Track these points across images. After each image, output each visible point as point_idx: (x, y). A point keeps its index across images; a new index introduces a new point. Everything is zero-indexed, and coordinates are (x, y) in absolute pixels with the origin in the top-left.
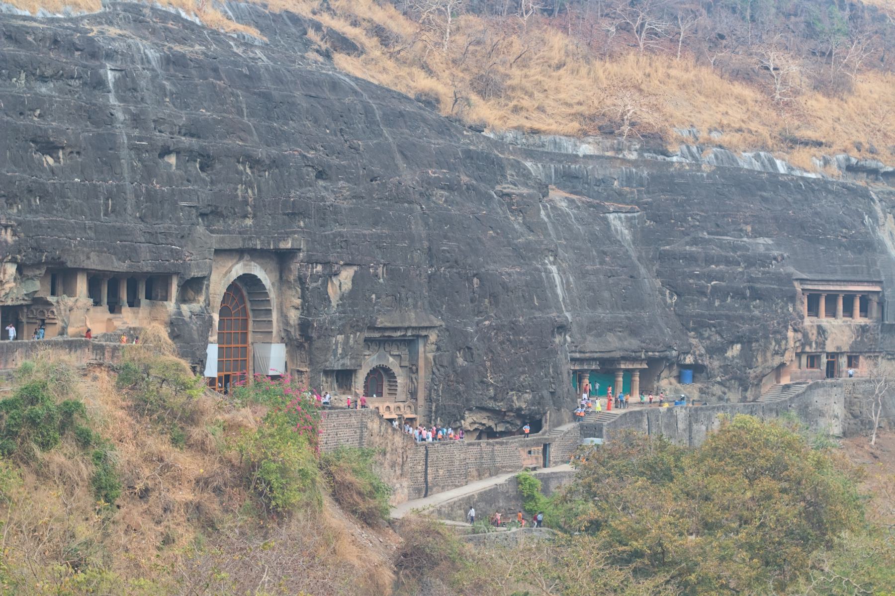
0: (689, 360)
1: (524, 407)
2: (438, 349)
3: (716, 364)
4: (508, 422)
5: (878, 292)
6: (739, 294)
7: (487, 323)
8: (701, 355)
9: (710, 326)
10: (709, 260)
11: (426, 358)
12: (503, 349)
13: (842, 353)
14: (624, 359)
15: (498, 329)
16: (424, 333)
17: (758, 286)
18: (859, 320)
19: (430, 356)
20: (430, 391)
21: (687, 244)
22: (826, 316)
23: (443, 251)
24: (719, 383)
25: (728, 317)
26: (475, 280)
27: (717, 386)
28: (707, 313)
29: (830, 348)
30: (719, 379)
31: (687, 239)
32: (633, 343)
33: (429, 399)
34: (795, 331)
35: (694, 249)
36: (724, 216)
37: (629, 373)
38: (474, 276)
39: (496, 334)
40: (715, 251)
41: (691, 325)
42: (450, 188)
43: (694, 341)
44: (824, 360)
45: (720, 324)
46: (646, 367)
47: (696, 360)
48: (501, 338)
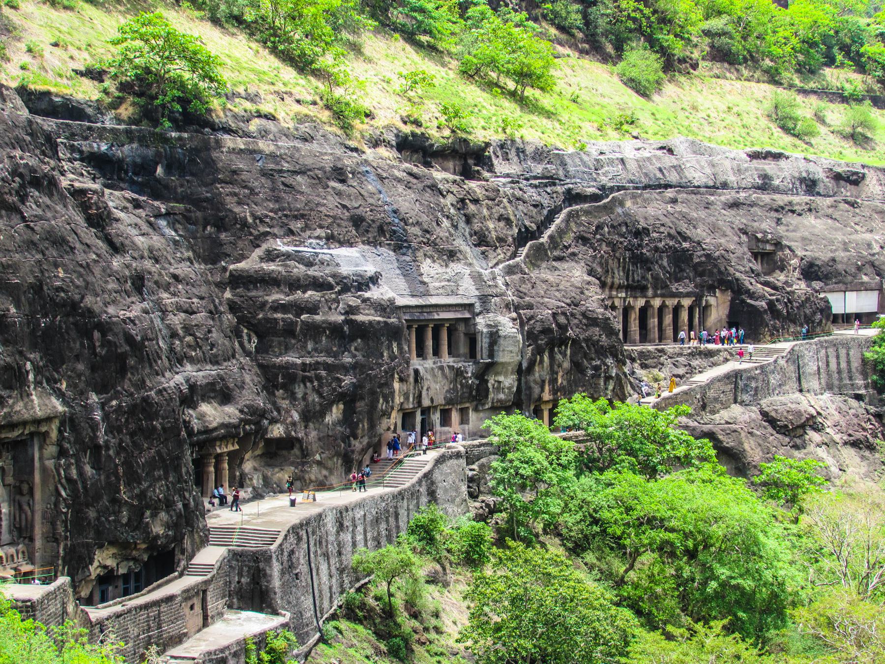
0: (277, 431)
1: (162, 532)
2: (62, 453)
3: (313, 434)
4: (135, 559)
5: (466, 320)
6: (335, 330)
7: (114, 403)
8: (294, 424)
9: (304, 380)
10: (295, 284)
11: (44, 469)
12: (134, 442)
13: (435, 407)
14: (224, 439)
15: (133, 410)
16: (44, 429)
17: (360, 318)
18: (447, 360)
19: (50, 464)
20: (53, 524)
21: (262, 259)
22: (418, 356)
23: (59, 289)
24: (319, 463)
25: (328, 367)
26: (97, 335)
27: (315, 468)
28: (299, 361)
29: (426, 403)
30: (318, 457)
31: (258, 252)
32: (230, 413)
33: (52, 538)
34: (401, 380)
35: (271, 267)
36: (296, 218)
37: (219, 458)
38: (94, 328)
39: (127, 420)
40: (299, 270)
41: (280, 380)
42: (36, 183)
43: (285, 404)
44: (419, 418)
45: (319, 378)
46: (237, 447)
47: (287, 432)
48: (132, 426)
